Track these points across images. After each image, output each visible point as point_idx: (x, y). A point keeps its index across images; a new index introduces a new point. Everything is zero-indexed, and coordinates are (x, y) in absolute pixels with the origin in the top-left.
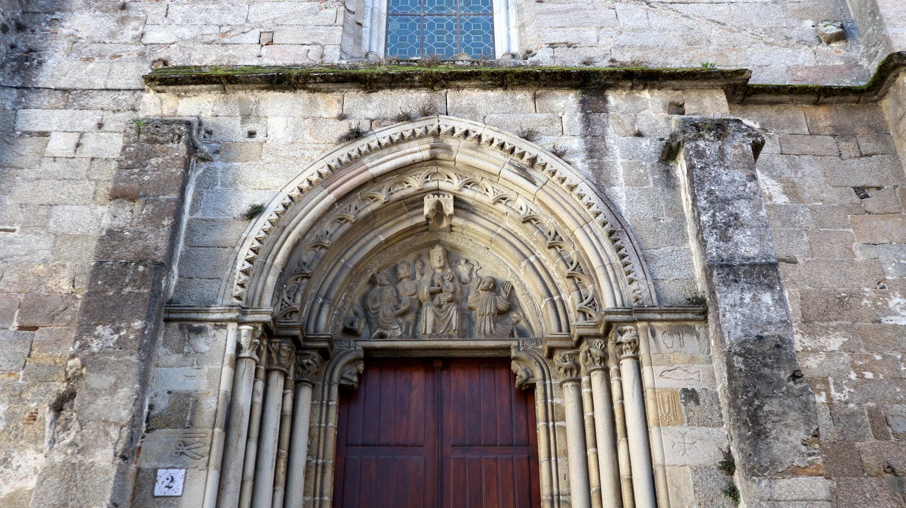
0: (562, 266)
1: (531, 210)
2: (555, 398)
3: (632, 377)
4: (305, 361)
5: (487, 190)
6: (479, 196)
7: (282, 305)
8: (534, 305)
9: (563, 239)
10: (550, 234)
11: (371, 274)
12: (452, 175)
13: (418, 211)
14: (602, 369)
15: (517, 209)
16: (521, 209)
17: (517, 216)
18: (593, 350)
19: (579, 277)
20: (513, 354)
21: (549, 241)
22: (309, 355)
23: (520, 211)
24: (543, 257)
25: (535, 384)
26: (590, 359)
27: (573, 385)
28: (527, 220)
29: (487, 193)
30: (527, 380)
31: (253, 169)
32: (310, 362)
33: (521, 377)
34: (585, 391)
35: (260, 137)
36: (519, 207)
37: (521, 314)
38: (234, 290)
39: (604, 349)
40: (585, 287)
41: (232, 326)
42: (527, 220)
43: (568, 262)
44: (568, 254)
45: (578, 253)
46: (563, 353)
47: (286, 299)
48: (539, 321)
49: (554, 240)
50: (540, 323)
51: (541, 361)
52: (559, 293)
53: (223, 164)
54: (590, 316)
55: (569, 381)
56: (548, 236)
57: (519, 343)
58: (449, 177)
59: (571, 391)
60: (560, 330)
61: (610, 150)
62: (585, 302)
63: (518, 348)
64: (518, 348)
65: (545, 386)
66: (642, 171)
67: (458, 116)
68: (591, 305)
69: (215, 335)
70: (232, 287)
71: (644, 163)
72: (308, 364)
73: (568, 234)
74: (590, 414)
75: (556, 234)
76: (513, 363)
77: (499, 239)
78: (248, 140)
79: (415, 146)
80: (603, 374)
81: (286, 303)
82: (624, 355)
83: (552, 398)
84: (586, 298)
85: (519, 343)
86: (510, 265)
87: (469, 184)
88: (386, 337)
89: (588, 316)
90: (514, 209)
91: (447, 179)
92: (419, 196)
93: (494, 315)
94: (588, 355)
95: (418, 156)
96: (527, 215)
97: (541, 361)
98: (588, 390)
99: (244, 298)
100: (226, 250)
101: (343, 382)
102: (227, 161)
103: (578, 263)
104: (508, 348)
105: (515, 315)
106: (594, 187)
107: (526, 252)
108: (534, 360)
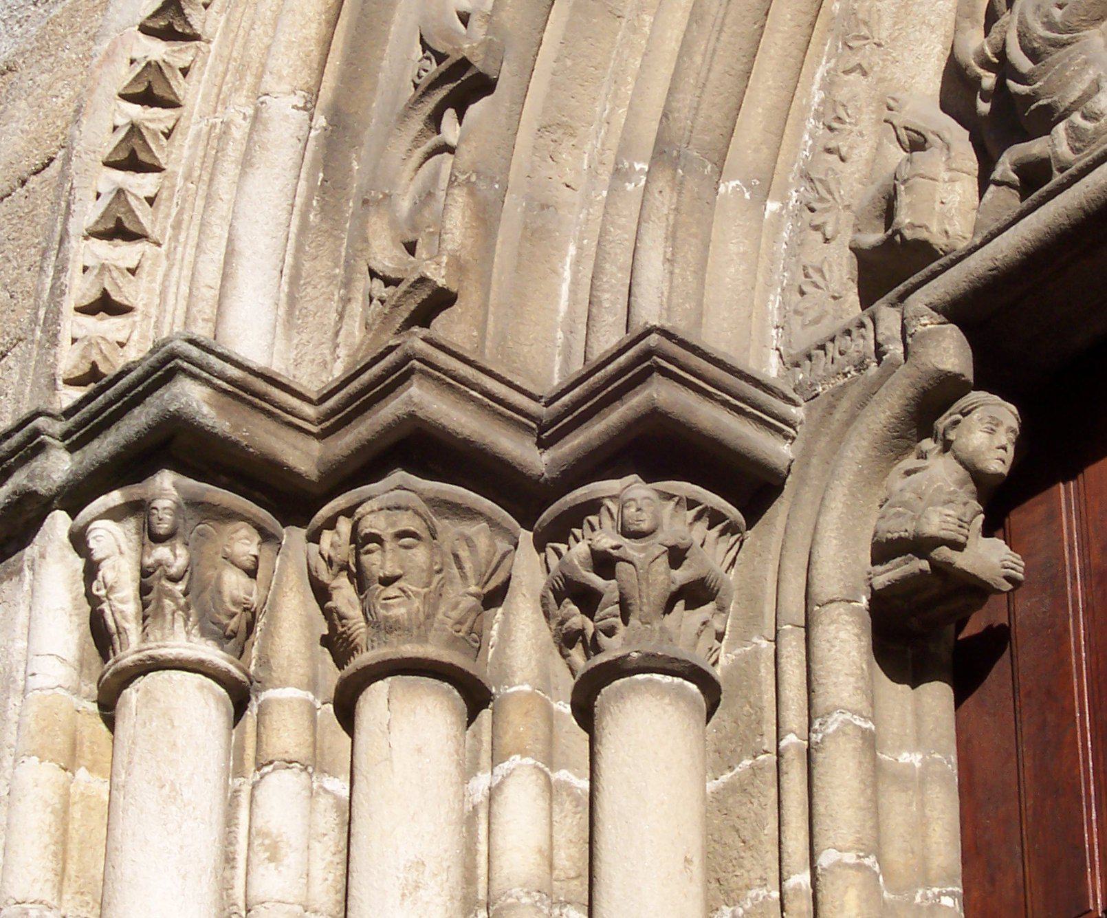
22: (594, 506)
32: (606, 540)
72: (604, 563)
88: (1048, 177)
101: (886, 575)
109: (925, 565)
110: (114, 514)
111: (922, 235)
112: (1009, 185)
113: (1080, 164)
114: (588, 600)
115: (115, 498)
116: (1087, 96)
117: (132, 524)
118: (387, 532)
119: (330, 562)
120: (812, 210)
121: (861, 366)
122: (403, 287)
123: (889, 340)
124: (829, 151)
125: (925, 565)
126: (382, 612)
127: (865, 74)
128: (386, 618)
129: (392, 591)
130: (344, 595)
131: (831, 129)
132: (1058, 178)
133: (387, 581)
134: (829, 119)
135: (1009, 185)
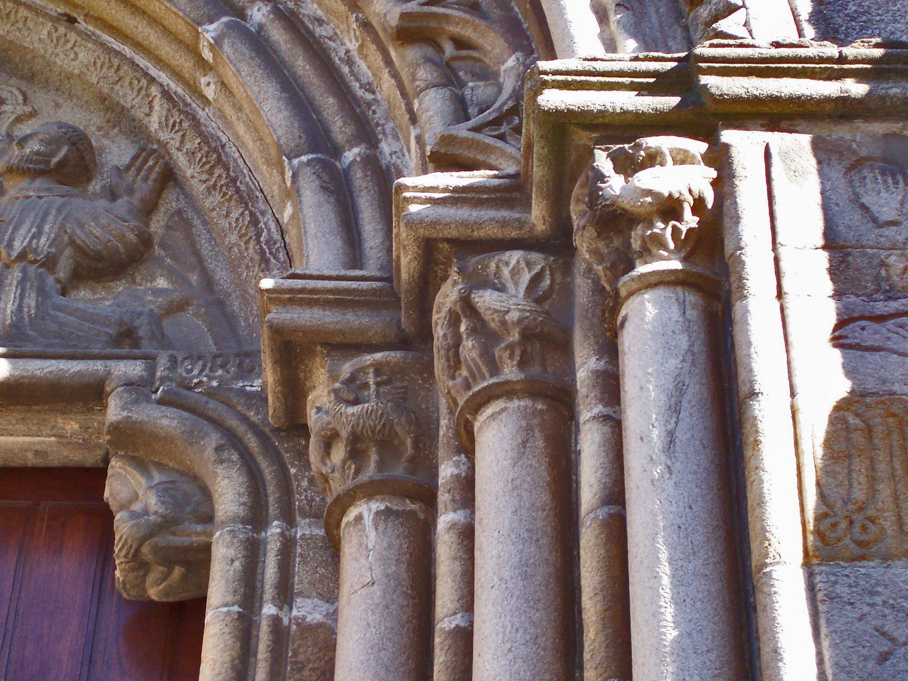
2: (299, 600)
8: (255, 222)
18: (485, 299)
25: (206, 550)
27: (387, 513)
30: (167, 524)
37: (194, 278)
46: (347, 368)
51: (252, 442)
55: (369, 491)
57: (152, 370)
68: (504, 128)
74: (458, 620)
83: (285, 595)
86: (163, 77)
93: (50, 263)
97: (252, 442)
105: (162, 283)
108: (214, 439)
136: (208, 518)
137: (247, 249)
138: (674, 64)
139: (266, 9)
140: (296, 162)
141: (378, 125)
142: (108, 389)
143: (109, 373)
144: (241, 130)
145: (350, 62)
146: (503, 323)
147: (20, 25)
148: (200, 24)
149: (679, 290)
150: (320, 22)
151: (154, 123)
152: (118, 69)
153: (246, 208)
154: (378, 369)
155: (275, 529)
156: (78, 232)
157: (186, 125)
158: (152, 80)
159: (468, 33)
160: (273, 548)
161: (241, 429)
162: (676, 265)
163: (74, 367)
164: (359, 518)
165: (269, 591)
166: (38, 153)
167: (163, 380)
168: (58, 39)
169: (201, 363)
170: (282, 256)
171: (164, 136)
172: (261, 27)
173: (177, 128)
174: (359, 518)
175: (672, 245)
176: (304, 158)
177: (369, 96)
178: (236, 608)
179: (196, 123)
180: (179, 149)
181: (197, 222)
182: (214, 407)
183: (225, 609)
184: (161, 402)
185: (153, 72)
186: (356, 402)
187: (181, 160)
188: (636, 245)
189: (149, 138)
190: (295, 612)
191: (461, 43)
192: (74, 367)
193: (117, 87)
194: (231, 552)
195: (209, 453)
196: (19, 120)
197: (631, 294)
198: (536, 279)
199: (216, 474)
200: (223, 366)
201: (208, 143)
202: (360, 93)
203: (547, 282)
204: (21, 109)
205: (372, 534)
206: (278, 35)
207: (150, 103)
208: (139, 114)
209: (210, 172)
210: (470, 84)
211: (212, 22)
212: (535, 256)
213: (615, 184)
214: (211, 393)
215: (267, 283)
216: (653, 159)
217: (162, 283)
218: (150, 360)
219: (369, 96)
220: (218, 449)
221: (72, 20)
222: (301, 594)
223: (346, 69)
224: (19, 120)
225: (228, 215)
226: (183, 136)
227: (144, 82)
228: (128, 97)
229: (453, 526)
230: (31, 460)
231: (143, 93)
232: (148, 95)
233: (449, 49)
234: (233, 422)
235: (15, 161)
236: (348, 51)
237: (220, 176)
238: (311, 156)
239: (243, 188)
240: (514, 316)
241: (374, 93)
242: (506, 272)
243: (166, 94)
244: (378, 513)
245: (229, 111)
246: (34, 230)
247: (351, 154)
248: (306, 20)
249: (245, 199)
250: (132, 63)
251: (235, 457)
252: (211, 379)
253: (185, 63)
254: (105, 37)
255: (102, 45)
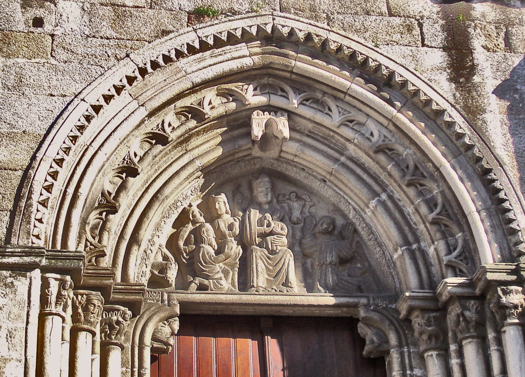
0: (424, 209)
1: (385, 137)
2: (414, 369)
3: (519, 347)
4: (115, 318)
5: (330, 110)
6: (319, 117)
7: (86, 246)
8: (384, 253)
9: (425, 174)
10: (407, 167)
11: (182, 208)
12: (288, 88)
13: (243, 130)
14: (477, 337)
15: (368, 135)
16: (372, 134)
17: (367, 144)
18: (467, 313)
19: (444, 222)
20: (362, 313)
21: (408, 178)
22: (118, 310)
23: (370, 137)
24: (398, 195)
26: (463, 324)
28: (380, 150)
29: (330, 113)
30: (380, 345)
31: (44, 69)
33: (372, 342)
34: (454, 362)
35: (48, 27)
36: (369, 132)
37: (367, 264)
38: (32, 227)
39: (480, 312)
40: (453, 235)
41: (36, 274)
42: (380, 150)
43: (431, 204)
44: (431, 191)
45: (442, 192)
47: (90, 239)
48: (391, 273)
49: (413, 176)
50: (393, 276)
52: (417, 240)
53: (4, 59)
54: (461, 271)
55: (434, 349)
56: (405, 170)
57: (369, 301)
58: (283, 90)
59: (436, 361)
60: (421, 286)
61: (479, 67)
62: (455, 254)
63: (367, 306)
64: (367, 306)
65: (402, 355)
66: (517, 96)
67: (297, 14)
68: (462, 258)
69: (12, 283)
70: (29, 223)
71: (518, 87)
72: (118, 322)
73: (432, 169)
75: (416, 167)
76: (360, 325)
77: (343, 171)
78: (32, 29)
79: (243, 49)
80: (477, 343)
81: (91, 244)
82: (509, 321)
83: (412, 369)
84: (455, 249)
85: (369, 301)
87: (307, 100)
88: (207, 290)
89: (458, 271)
90: (363, 135)
91: (280, 93)
92: (244, 113)
93: (335, 265)
94: (461, 319)
95: (248, 62)
96: (380, 143)
98: (458, 361)
99: (43, 237)
100: (16, 173)
101: (156, 345)
102: (8, 56)
103: (444, 206)
104: (355, 306)
105: (359, 265)
106: (463, 113)
107: (377, 188)
108: (387, 323)
109: (166, 347)
110: (56, 279)
111: (169, 279)
112: (197, 285)
113: (214, 292)
114: (112, 328)
115: (58, 276)
116: (218, 279)
117: (58, 282)
118: (97, 305)
119: (80, 303)
120: (145, 260)
121: (158, 301)
122: (97, 249)
123: (166, 300)
124: (150, 250)
125: (166, 347)
126: (89, 319)
127: (159, 237)
128: (90, 320)
129: (92, 315)
130: (80, 310)
131: (152, 246)
132: (209, 291)
133: (92, 313)
134: (152, 243)
135: (197, 285)
136: (387, 342)
137: (382, 261)
138: (515, 267)
139: (386, 195)
140: (402, 249)
141: (420, 237)
142: (359, 306)
143: (359, 302)
144: (379, 227)
145: (409, 215)
146: (472, 320)
147: (311, 181)
148: (371, 200)
149: (517, 326)
150: (399, 200)
151: (351, 216)
152: (340, 199)
153: (381, 249)
154: (434, 317)
155: (406, 350)
156: (340, 253)
157: (361, 219)
158: (350, 203)
159: (448, 223)
160: (406, 355)
161: (393, 319)
162: (517, 321)
163: (351, 300)
164: (432, 355)
165: (408, 368)
166: (326, 228)
167: (372, 304)
168: (322, 187)
169: (380, 299)
170: (392, 265)
171: (354, 221)
172: (384, 201)
173: (358, 219)
174: (432, 355)
175: (516, 315)
176: (404, 248)
177: (416, 227)
178: (401, 372)
179: (364, 220)
180: (359, 225)
181: (363, 245)
182: (385, 312)
183: (399, 372)
184: (373, 310)
185: (350, 201)
186: (429, 326)
187: (360, 229)
188: (507, 313)
189: (349, 219)
190: (414, 373)
191: (446, 226)
192: (351, 300)
193: (340, 203)
194: (398, 356)
195: (387, 326)
196: (311, 207)
197: (507, 326)
198: (477, 307)
199: (389, 333)
200: (385, 300)
201: (367, 226)
202: (413, 226)
203: (479, 309)
204: (311, 204)
205: (436, 360)
206: (389, 204)
207: (350, 210)
208: (347, 213)
209: (369, 235)
210: (449, 238)
211: (373, 200)
212: (477, 302)
213: (504, 300)
214: (383, 308)
215: (407, 294)
216: (511, 291)
217: (359, 265)
218: (368, 297)
219: (416, 227)
220: (389, 325)
221: (325, 181)
222: (415, 368)
223: (408, 217)
224: (311, 207)
225: (375, 249)
226: (360, 222)
227: (347, 204)
228: (343, 207)
229: (457, 363)
230: (334, 316)
231: (347, 207)
232: (349, 208)
233: (443, 227)
234: (391, 317)
235: (320, 230)
236: (408, 211)
237: (372, 237)
238: (406, 247)
239: (379, 242)
240: (474, 319)
241: (417, 226)
242: (471, 305)
243: (354, 209)
244: (437, 355)
245: (375, 221)
246: (331, 255)
247: (414, 246)
248: (396, 199)
249: (380, 245)
250: (344, 198)
251: (393, 328)
252: (383, 304)
253: (362, 205)
254: (335, 188)
255: (334, 190)
